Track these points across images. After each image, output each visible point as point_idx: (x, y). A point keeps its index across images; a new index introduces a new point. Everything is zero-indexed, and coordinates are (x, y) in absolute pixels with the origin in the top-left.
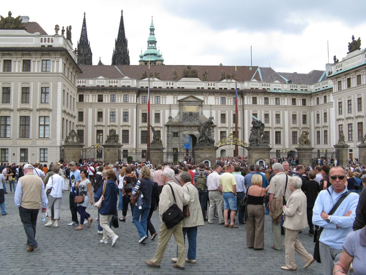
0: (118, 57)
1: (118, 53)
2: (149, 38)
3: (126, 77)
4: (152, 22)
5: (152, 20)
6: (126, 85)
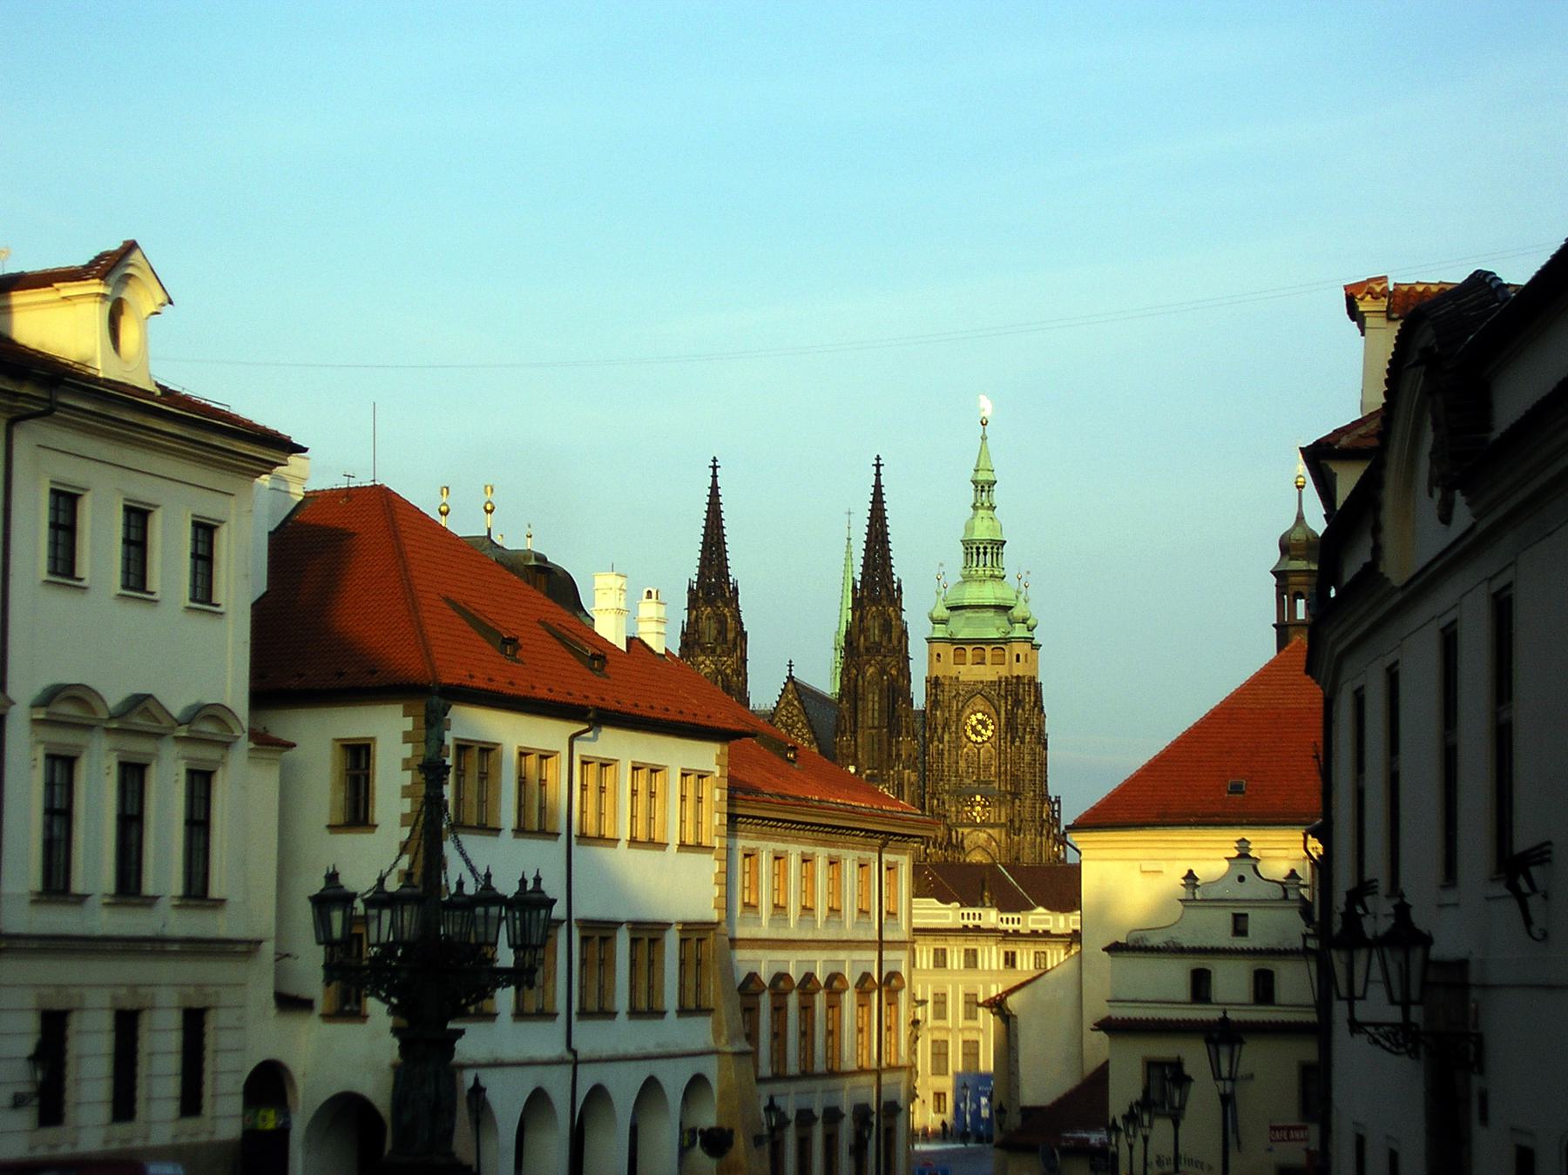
0: (868, 662)
1: (867, 649)
2: (969, 528)
3: (1041, 910)
4: (983, 451)
5: (984, 438)
6: (1040, 928)
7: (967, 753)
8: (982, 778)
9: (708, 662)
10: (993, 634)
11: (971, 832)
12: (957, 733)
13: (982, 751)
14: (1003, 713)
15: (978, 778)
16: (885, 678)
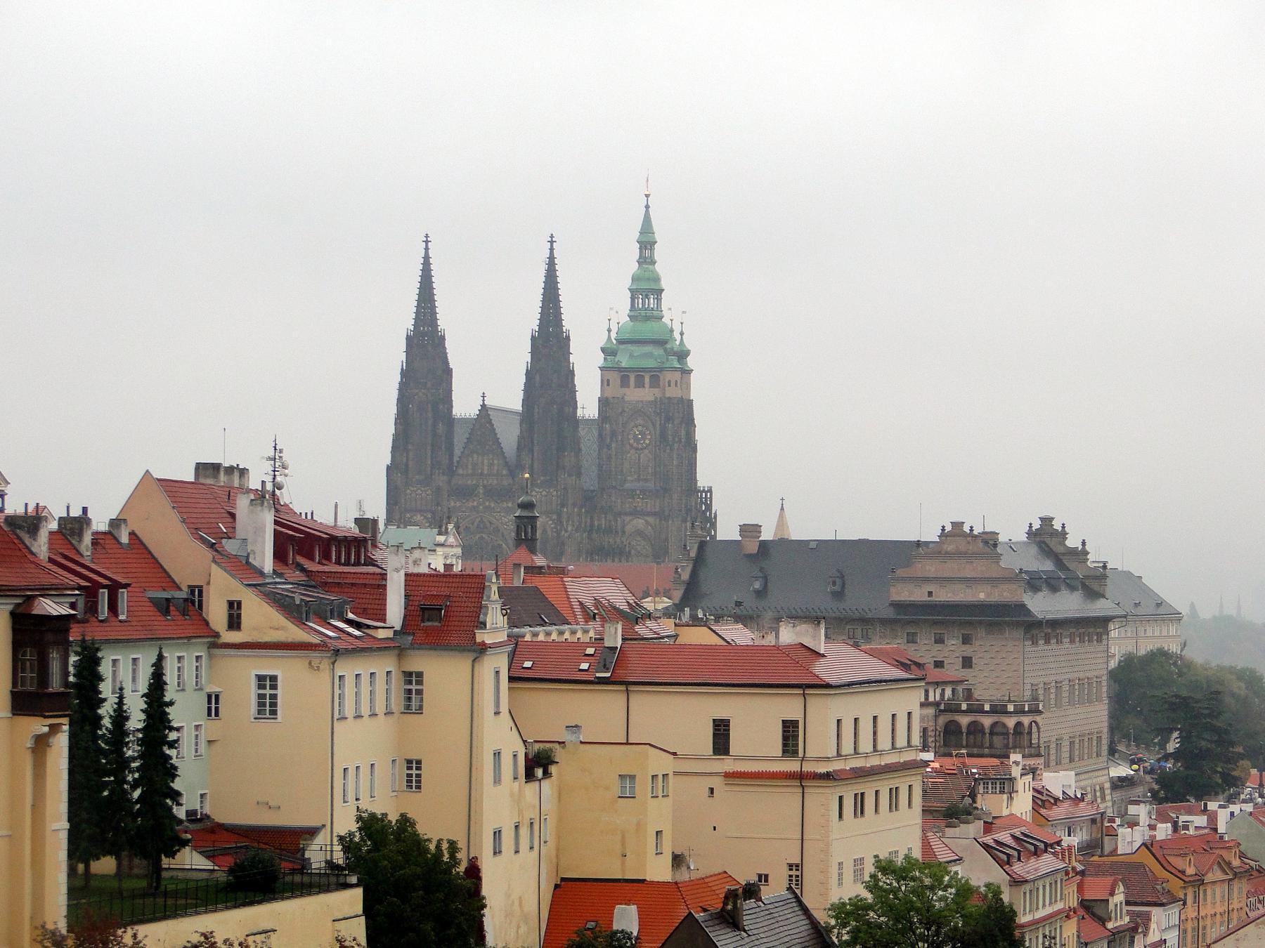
4: (647, 220)
7: (630, 457)
8: (642, 477)
9: (421, 394)
10: (651, 363)
11: (631, 520)
12: (622, 441)
13: (642, 456)
14: (658, 426)
15: (639, 476)
16: (555, 406)
